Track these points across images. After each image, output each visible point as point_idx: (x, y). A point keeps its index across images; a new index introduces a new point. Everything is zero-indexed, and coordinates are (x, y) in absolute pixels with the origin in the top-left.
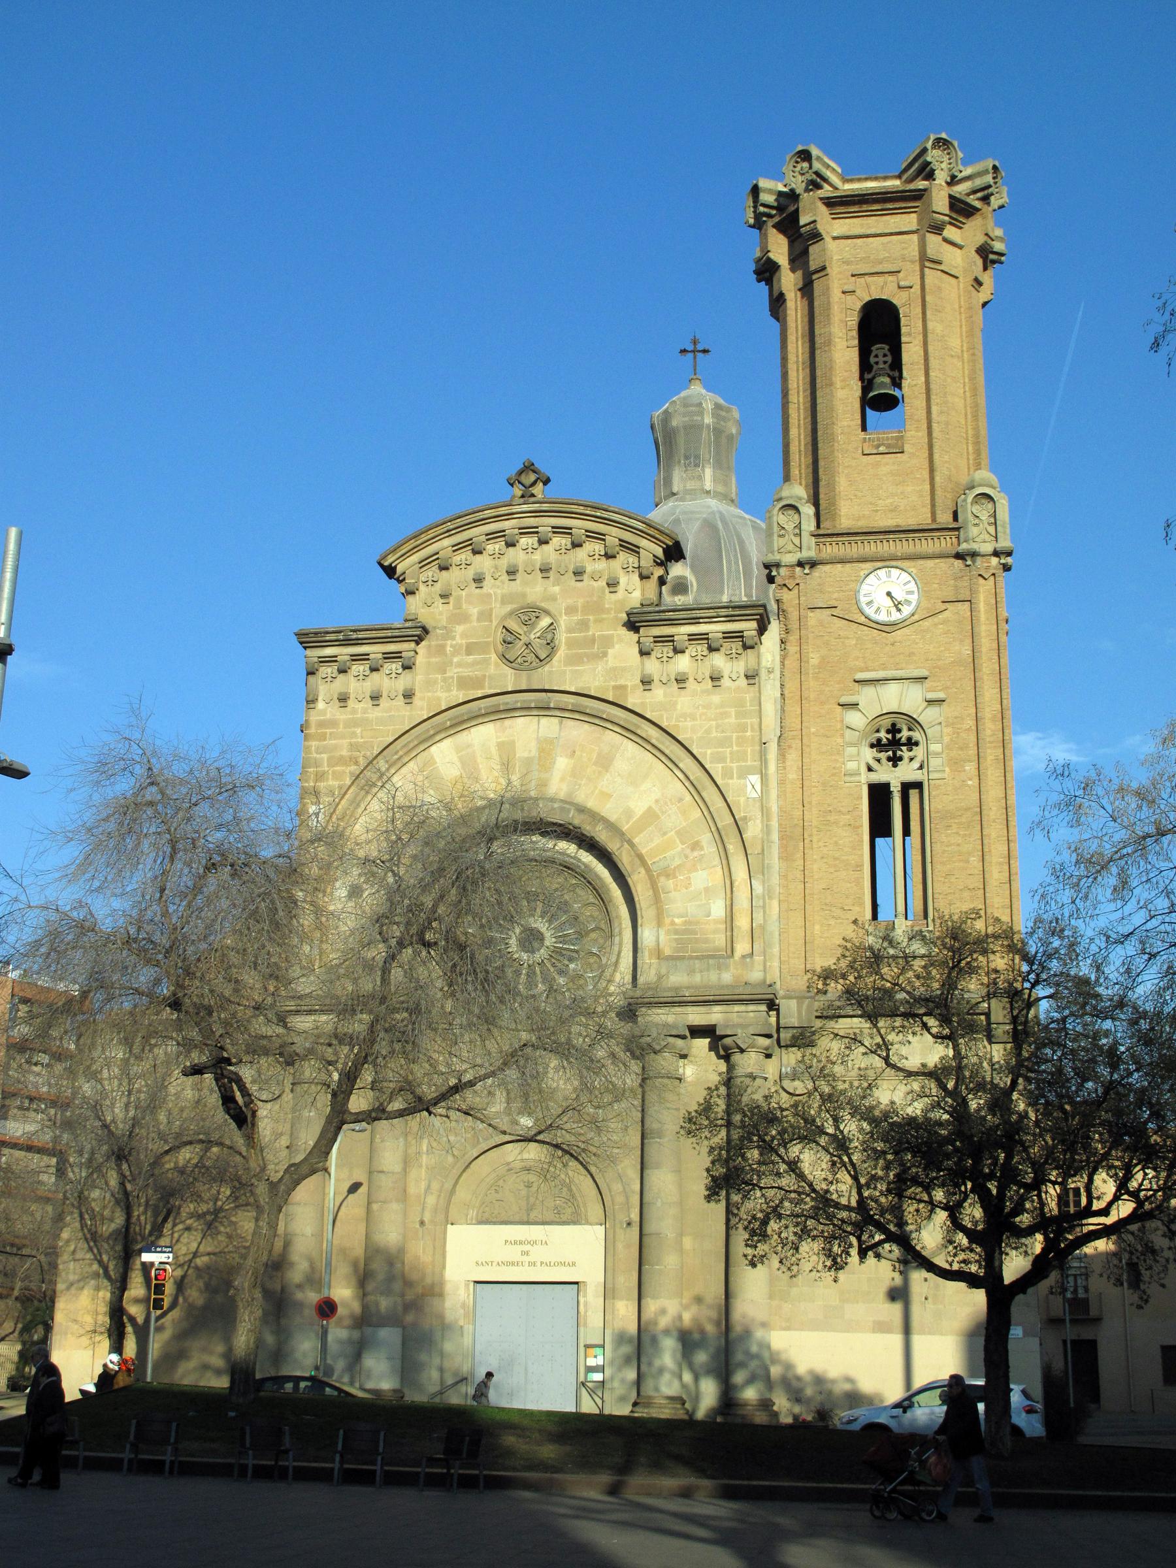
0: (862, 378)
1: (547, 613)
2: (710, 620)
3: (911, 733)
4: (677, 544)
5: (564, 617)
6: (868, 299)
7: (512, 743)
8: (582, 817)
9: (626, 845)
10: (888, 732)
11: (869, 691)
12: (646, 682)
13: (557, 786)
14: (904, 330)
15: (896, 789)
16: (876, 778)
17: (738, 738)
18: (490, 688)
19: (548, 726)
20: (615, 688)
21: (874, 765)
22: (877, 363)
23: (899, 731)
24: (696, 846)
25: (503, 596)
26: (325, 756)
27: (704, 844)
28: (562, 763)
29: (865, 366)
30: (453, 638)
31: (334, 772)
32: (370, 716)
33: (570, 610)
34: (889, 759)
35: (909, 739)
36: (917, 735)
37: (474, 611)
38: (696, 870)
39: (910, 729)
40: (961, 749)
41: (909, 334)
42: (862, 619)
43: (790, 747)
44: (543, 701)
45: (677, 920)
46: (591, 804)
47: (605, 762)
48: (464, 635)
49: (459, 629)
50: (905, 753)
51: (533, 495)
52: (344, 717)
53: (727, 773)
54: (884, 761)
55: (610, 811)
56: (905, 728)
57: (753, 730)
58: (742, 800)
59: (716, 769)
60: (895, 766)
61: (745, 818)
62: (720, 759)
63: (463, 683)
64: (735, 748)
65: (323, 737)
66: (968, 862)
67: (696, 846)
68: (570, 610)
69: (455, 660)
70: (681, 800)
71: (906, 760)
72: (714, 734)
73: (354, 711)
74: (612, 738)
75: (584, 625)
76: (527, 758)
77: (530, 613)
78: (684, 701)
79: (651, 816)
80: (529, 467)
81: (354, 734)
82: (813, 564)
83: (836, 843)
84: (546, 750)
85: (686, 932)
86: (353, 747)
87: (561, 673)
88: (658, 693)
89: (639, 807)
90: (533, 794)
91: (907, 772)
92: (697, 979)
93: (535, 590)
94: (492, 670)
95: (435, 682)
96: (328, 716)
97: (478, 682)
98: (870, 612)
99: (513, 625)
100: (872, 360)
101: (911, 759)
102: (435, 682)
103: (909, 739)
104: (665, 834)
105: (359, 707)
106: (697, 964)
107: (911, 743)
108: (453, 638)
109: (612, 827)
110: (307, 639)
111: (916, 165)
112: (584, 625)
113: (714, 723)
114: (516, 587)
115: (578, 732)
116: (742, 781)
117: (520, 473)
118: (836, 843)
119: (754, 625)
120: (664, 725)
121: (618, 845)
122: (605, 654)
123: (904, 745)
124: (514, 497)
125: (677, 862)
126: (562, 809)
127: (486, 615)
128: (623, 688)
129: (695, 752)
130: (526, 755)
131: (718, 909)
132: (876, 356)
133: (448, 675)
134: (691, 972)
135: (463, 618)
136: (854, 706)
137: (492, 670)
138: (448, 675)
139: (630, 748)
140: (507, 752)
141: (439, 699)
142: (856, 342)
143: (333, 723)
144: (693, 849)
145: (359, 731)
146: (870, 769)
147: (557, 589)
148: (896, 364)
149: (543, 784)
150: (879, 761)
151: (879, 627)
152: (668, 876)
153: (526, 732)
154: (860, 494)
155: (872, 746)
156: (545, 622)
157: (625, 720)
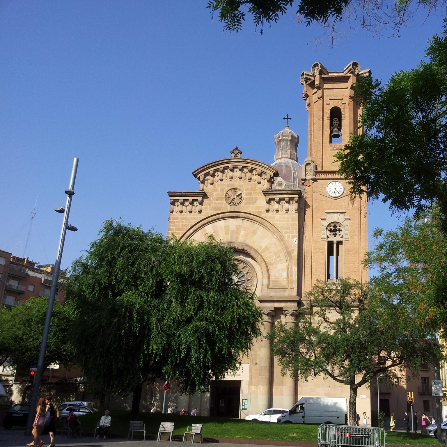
0: (330, 129)
1: (240, 190)
2: (285, 194)
3: (340, 228)
4: (277, 172)
5: (245, 191)
6: (333, 106)
7: (229, 226)
8: (247, 247)
9: (259, 256)
10: (333, 227)
11: (329, 216)
12: (268, 211)
13: (241, 239)
14: (342, 116)
15: (335, 243)
16: (329, 239)
17: (292, 227)
18: (223, 210)
19: (239, 221)
20: (258, 212)
21: (329, 236)
22: (335, 124)
23: (337, 227)
24: (279, 257)
25: (228, 185)
27: (281, 257)
28: (242, 232)
29: (331, 125)
30: (213, 196)
33: (247, 190)
34: (333, 234)
35: (339, 229)
36: (341, 228)
37: (219, 188)
38: (279, 264)
39: (339, 227)
40: (353, 232)
41: (344, 117)
42: (328, 196)
44: (237, 215)
45: (273, 278)
46: (250, 244)
47: (254, 232)
48: (216, 195)
49: (215, 193)
50: (337, 233)
51: (237, 157)
53: (289, 237)
54: (332, 235)
56: (338, 226)
58: (292, 245)
60: (335, 236)
62: (287, 233)
63: (215, 209)
65: (174, 222)
66: (354, 264)
67: (279, 257)
68: (247, 190)
69: (213, 202)
71: (338, 235)
72: (285, 226)
73: (184, 215)
74: (257, 226)
75: (250, 194)
76: (233, 231)
77: (234, 189)
78: (277, 216)
79: (267, 248)
80: (237, 149)
81: (183, 222)
82: (315, 180)
83: (318, 257)
84: (238, 228)
85: (275, 281)
86: (183, 225)
87: (243, 207)
88: (270, 213)
89: (263, 245)
90: (234, 241)
92: (278, 294)
93: (236, 183)
94: (224, 205)
95: (207, 208)
96: (176, 216)
97: (219, 209)
98: (330, 194)
100: (333, 123)
101: (339, 235)
102: (207, 208)
103: (339, 229)
104: (271, 253)
105: (186, 214)
107: (340, 230)
108: (213, 196)
109: (256, 251)
110: (171, 194)
111: (348, 69)
112: (250, 194)
113: (285, 223)
114: (232, 182)
115: (247, 223)
116: (292, 239)
117: (234, 150)
118: (318, 257)
119: (297, 196)
122: (256, 202)
123: (338, 231)
124: (232, 157)
125: (274, 261)
126: (242, 245)
127: (222, 190)
128: (261, 212)
130: (232, 230)
131: (285, 275)
132: (335, 122)
133: (211, 206)
134: (276, 292)
135: (216, 190)
136: (325, 219)
137: (224, 205)
138: (211, 206)
139: (261, 228)
140: (227, 228)
141: (208, 213)
142: (329, 118)
143: (177, 218)
144: (278, 258)
145: (185, 221)
146: (328, 237)
147: (243, 183)
148: (340, 125)
149: (237, 238)
150: (331, 235)
151: (332, 198)
152: (271, 265)
153: (232, 223)
154: (328, 161)
155: (329, 231)
157: (261, 221)
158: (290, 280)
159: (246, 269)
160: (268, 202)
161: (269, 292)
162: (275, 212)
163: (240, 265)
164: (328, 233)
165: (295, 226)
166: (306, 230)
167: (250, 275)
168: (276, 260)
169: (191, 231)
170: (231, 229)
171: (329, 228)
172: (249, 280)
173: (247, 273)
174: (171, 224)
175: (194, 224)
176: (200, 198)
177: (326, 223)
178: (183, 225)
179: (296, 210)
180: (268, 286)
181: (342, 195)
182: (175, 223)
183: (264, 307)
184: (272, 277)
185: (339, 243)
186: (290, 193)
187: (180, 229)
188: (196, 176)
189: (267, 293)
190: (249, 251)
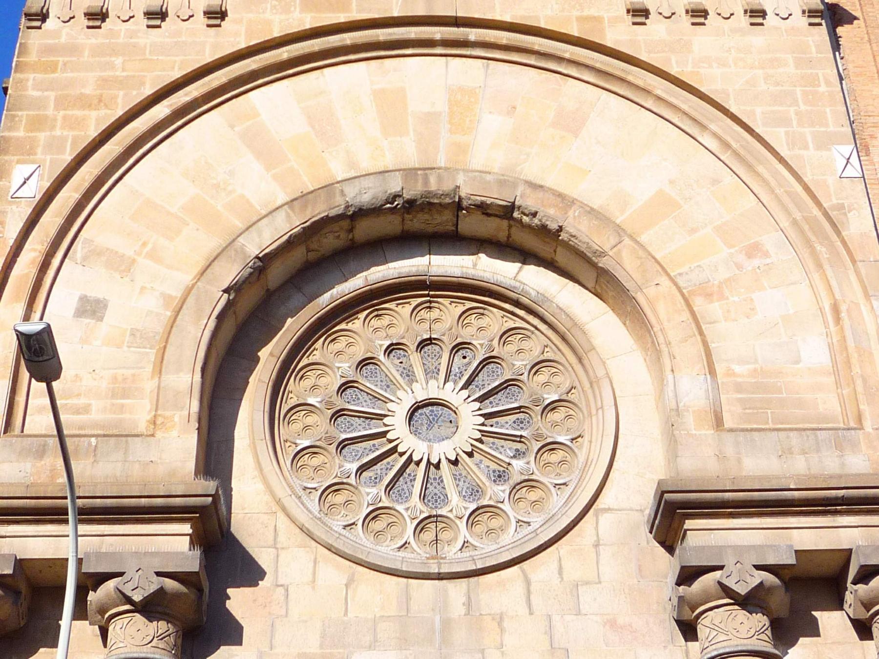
8: (540, 194)
9: (627, 241)
18: (359, 11)
19: (465, 71)
20: (580, 19)
24: (754, 250)
26: (52, 95)
31: (65, 118)
32: (142, 41)
43: (872, 137)
45: (737, 369)
47: (571, 124)
52: (93, 41)
55: (590, 191)
57: (828, 83)
59: (777, 137)
61: (841, 207)
64: (803, 107)
67: (754, 250)
70: (715, 182)
78: (704, 40)
79: (663, 205)
81: (111, 66)
84: (462, 107)
86: (104, 82)
96: (63, 40)
104: (693, 231)
106: (795, 439)
120: (674, 71)
121: (613, 241)
125: (723, 274)
128: (598, 20)
129: (733, 109)
131: (815, 351)
134: (786, 452)
143: (73, 49)
144: (749, 256)
145: (118, 61)
152: (709, 296)
153: (424, 79)
158: (865, 381)
159: (525, 345)
161: (730, 451)
162: (687, 20)
163: (484, 322)
165: (823, 88)
166: (872, 137)
167: (556, 380)
168: (739, 267)
169: (161, 110)
172: (552, 407)
173: (537, 366)
174: (32, 76)
175: (177, 74)
178: (104, 82)
179: (812, 13)
180: (719, 422)
182: (54, 71)
183: (721, 549)
187: (84, 102)
189: (721, 457)
190: (552, 212)
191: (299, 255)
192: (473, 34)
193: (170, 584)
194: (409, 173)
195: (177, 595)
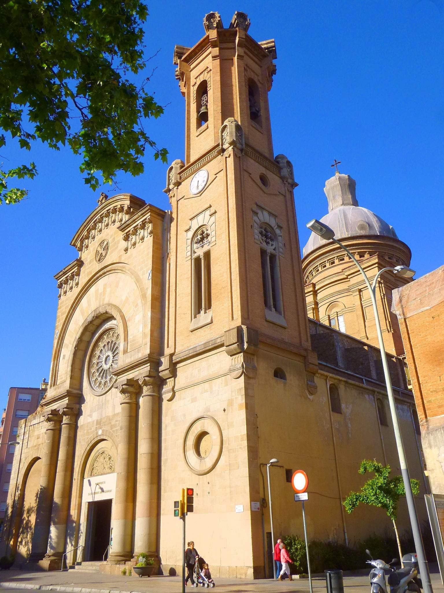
24: (137, 306)
49: (89, 256)
75: (114, 239)
89: (124, 298)
91: (206, 248)
97: (90, 272)
99: (99, 249)
107: (208, 235)
112: (114, 239)
149: (104, 300)
155: (196, 243)
156: (105, 243)
160: (126, 238)
164: (195, 246)
170: (100, 291)
171: (195, 240)
176: (75, 269)
177: (190, 234)
181: (206, 185)
184: (130, 337)
185: (207, 255)
186: (142, 215)
188: (74, 245)
189: (123, 361)
191: (88, 334)
192: (105, 270)
193: (65, 409)
194: (95, 311)
195: (67, 411)
